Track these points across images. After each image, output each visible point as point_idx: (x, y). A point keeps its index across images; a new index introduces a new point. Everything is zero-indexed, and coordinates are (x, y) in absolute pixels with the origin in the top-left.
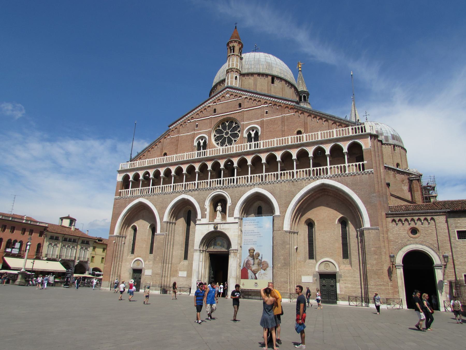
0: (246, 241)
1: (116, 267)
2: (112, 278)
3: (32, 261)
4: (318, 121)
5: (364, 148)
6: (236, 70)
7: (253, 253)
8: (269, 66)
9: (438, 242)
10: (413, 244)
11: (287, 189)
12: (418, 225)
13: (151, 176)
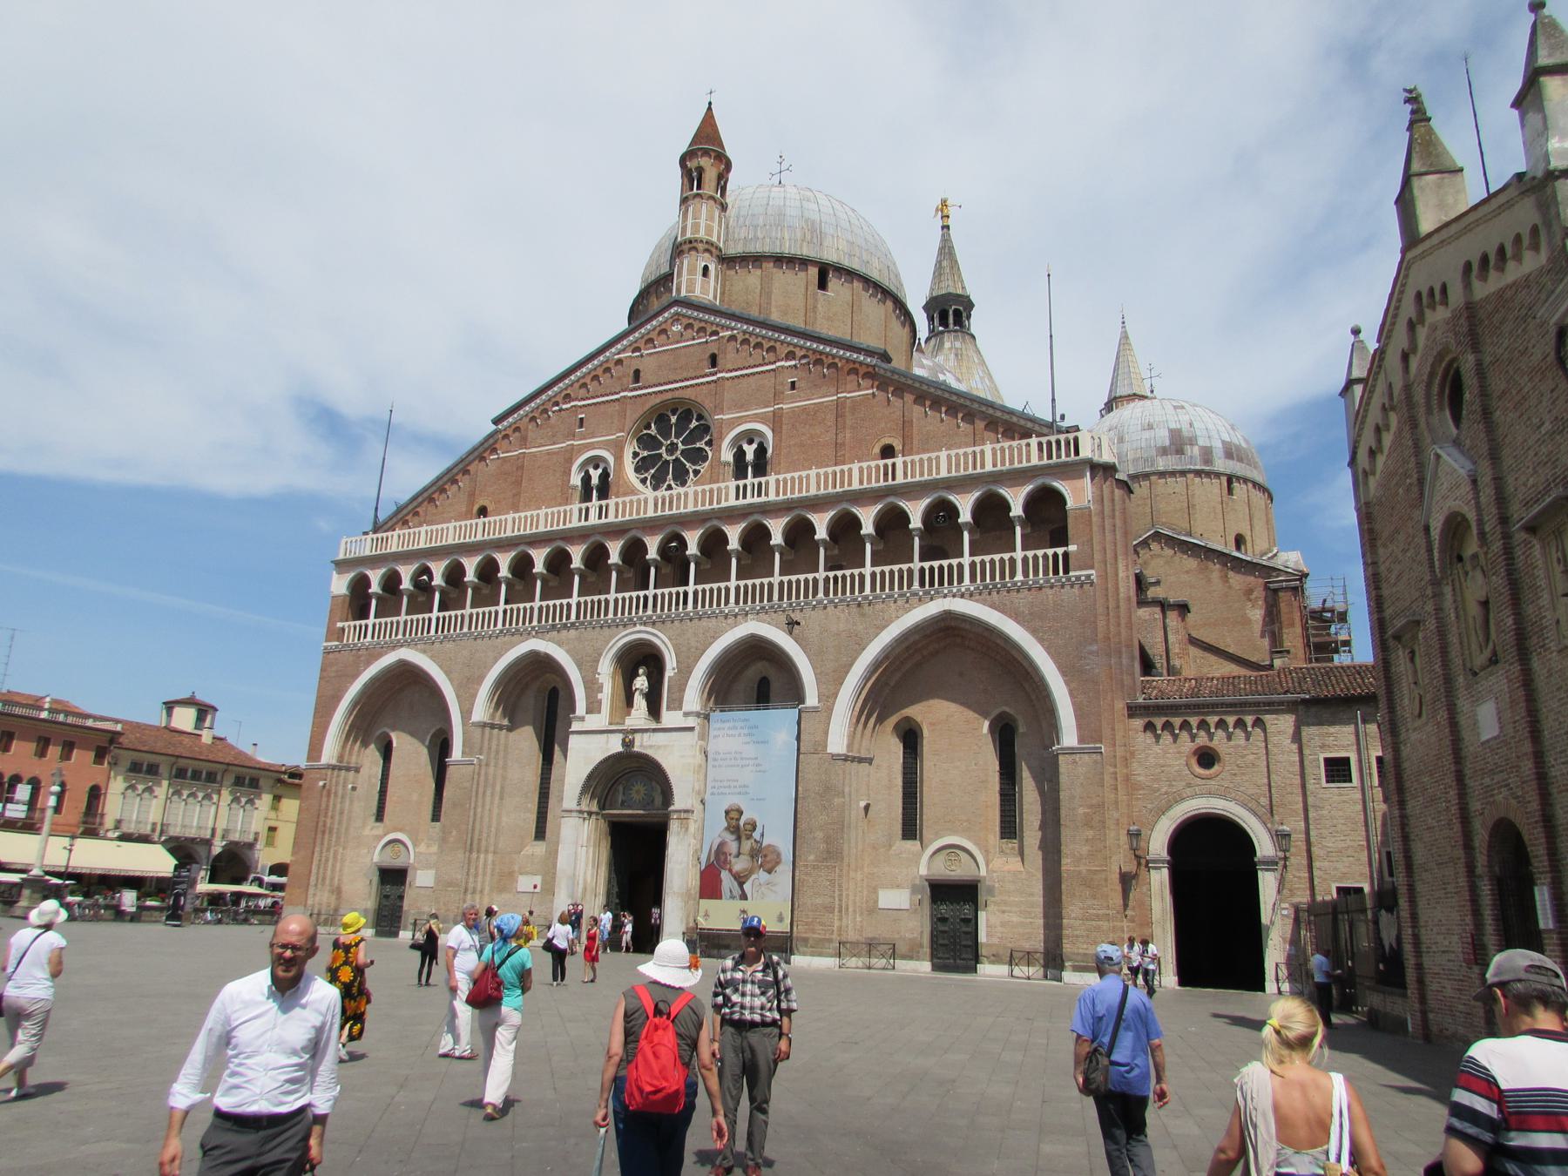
0: (717, 784)
1: (327, 860)
2: (314, 895)
3: (66, 841)
4: (943, 415)
5: (1070, 504)
6: (706, 246)
7: (738, 820)
8: (813, 231)
9: (1270, 791)
10: (1201, 795)
11: (842, 626)
12: (1219, 741)
13: (438, 580)
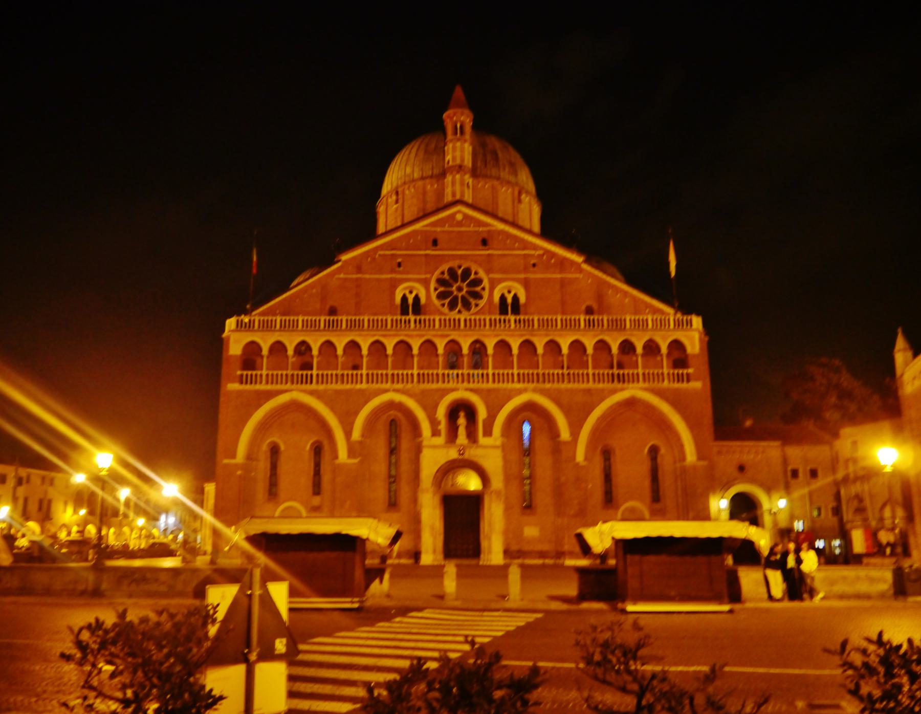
5: (689, 350)
